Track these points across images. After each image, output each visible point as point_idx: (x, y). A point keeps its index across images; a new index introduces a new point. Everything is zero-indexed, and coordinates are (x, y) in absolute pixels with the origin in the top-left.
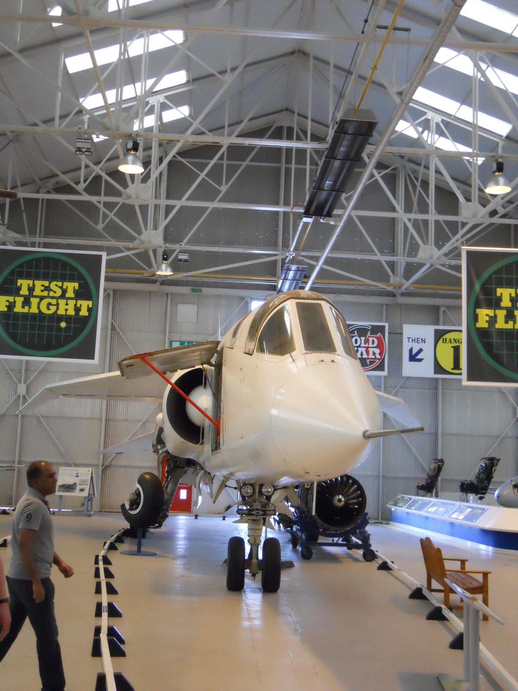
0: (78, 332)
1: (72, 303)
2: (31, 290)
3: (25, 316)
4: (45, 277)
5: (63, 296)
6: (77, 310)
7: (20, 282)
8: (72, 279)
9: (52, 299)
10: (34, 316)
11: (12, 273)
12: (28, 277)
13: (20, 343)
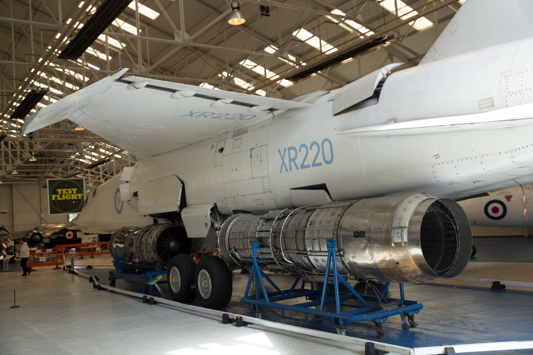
0: (79, 204)
1: (76, 195)
2: (62, 192)
3: (61, 201)
4: (66, 188)
5: (72, 193)
6: (78, 197)
7: (58, 190)
8: (74, 187)
9: (69, 194)
10: (64, 201)
11: (55, 187)
12: (60, 188)
13: (62, 210)
